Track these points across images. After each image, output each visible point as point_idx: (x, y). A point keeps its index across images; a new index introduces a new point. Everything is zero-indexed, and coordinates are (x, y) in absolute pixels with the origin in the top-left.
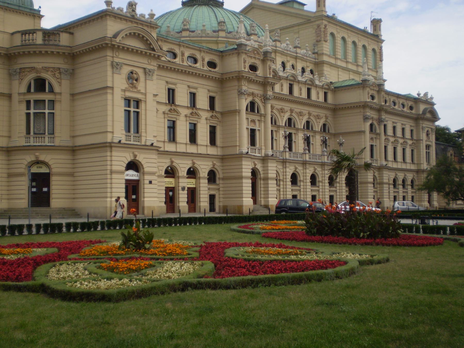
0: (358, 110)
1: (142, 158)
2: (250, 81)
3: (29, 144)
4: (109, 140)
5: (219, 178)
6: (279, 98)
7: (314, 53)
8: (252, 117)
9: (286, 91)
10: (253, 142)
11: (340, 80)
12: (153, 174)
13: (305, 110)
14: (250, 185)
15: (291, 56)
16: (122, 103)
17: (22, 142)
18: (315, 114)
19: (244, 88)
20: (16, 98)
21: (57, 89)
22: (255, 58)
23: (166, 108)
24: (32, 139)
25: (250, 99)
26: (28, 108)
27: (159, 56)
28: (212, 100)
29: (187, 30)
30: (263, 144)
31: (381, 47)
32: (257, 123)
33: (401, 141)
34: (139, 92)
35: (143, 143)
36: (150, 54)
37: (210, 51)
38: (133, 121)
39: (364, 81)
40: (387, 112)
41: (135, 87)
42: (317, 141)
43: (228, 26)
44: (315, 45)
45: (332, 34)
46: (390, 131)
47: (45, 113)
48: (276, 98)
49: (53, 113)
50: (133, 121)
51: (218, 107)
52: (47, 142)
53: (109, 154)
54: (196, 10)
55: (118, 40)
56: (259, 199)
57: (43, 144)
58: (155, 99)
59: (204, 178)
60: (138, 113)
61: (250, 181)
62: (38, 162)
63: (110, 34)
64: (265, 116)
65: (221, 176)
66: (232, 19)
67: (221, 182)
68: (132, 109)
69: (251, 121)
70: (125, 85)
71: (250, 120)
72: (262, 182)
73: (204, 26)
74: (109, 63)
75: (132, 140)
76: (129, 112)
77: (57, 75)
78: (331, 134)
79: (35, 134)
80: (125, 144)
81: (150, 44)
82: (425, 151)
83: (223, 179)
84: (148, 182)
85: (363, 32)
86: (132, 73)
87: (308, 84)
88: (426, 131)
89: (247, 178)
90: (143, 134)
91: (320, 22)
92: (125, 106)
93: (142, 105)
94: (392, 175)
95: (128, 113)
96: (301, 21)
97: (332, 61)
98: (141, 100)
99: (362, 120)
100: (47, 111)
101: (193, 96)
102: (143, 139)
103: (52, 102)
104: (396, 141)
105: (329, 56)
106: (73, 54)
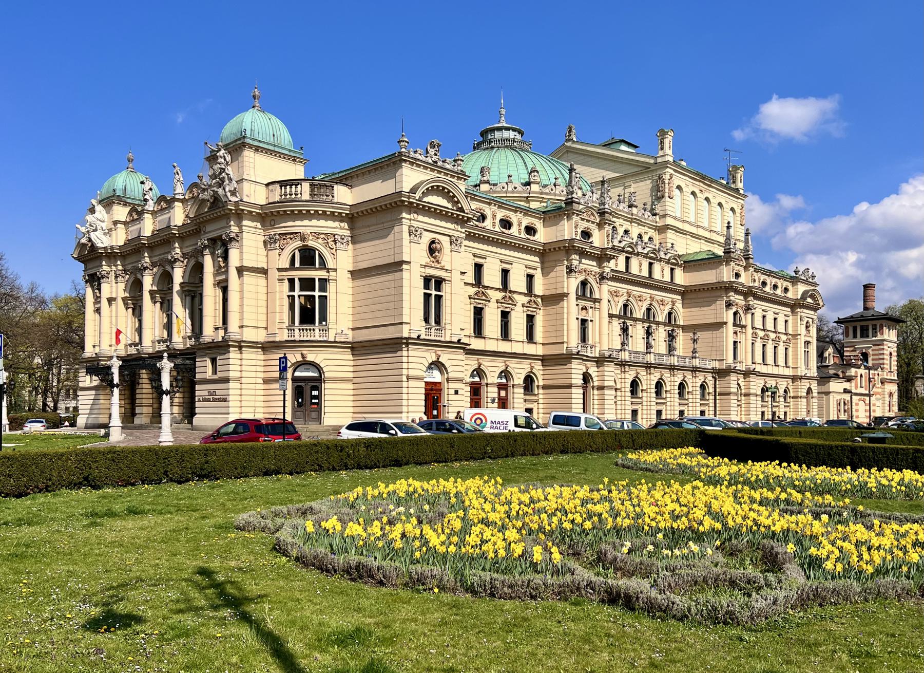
1: (446, 357)
2: (583, 254)
3: (293, 339)
4: (406, 335)
5: (538, 387)
6: (617, 277)
8: (583, 303)
9: (622, 267)
10: (584, 338)
11: (689, 252)
12: (460, 380)
13: (646, 292)
15: (626, 219)
16: (421, 283)
17: (283, 336)
19: (575, 263)
20: (274, 275)
21: (330, 265)
22: (588, 221)
23: (472, 291)
24: (297, 330)
25: (582, 278)
26: (292, 288)
27: (468, 218)
28: (530, 278)
29: (488, 182)
30: (597, 340)
32: (590, 310)
33: (773, 336)
34: (442, 269)
35: (448, 339)
36: (458, 215)
37: (527, 212)
38: (433, 308)
40: (757, 297)
41: (437, 261)
42: (661, 334)
43: (542, 177)
45: (679, 187)
47: (314, 296)
48: (613, 279)
49: (326, 297)
50: (433, 308)
51: (539, 289)
52: (317, 336)
53: (405, 353)
54: (497, 154)
55: (417, 196)
57: (312, 339)
58: (462, 277)
59: (519, 386)
60: (439, 298)
61: (581, 391)
62: (305, 364)
63: (406, 188)
65: (541, 383)
66: (547, 168)
67: (541, 391)
68: (434, 293)
69: (582, 309)
70: (425, 258)
72: (596, 392)
73: (510, 176)
74: (405, 229)
75: (433, 334)
76: (431, 295)
77: (331, 244)
78: (679, 326)
79: (301, 322)
80: (425, 340)
81: (458, 202)
82: (803, 350)
83: (544, 387)
84: (452, 392)
86: (433, 242)
87: (651, 258)
88: (805, 323)
89: (577, 386)
90: (447, 327)
92: (425, 288)
93: (446, 287)
95: (427, 297)
96: (636, 169)
97: (679, 225)
98: (444, 280)
100: (317, 293)
101: (505, 273)
102: (448, 333)
103: (324, 282)
104: (765, 338)
105: (675, 218)
106: (353, 214)
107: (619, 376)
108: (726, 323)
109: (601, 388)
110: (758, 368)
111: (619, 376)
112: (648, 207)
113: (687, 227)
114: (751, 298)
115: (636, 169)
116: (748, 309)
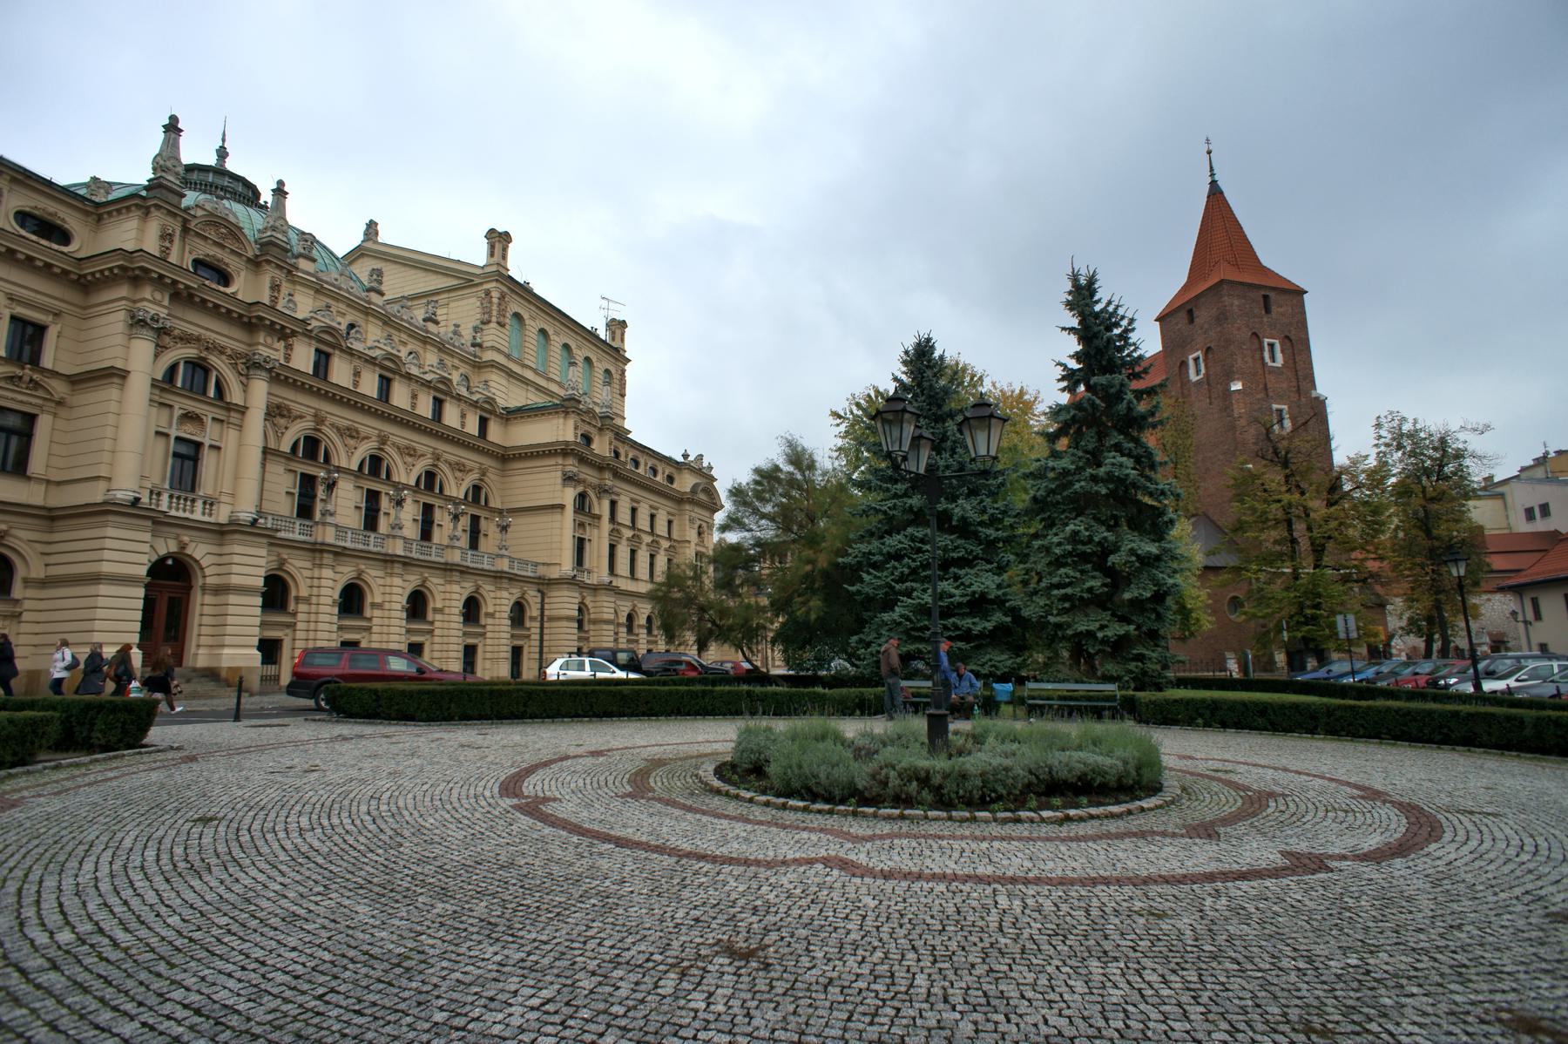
0: (552, 461)
7: (474, 345)
14: (140, 604)
18: (452, 459)
31: (623, 371)
39: (572, 399)
40: (617, 475)
44: (476, 329)
45: (517, 316)
46: (624, 516)
56: (193, 650)
64: (242, 410)
65: (38, 572)
71: (177, 413)
72: (208, 599)
78: (493, 510)
85: (590, 335)
91: (494, 284)
94: (625, 608)
96: (456, 282)
99: (559, 481)
105: (508, 356)
107: (307, 573)
108: (562, 507)
109: (222, 590)
110: (624, 584)
111: (307, 573)
112: (467, 334)
113: (529, 375)
114: (607, 475)
115: (456, 282)
116: (602, 491)
